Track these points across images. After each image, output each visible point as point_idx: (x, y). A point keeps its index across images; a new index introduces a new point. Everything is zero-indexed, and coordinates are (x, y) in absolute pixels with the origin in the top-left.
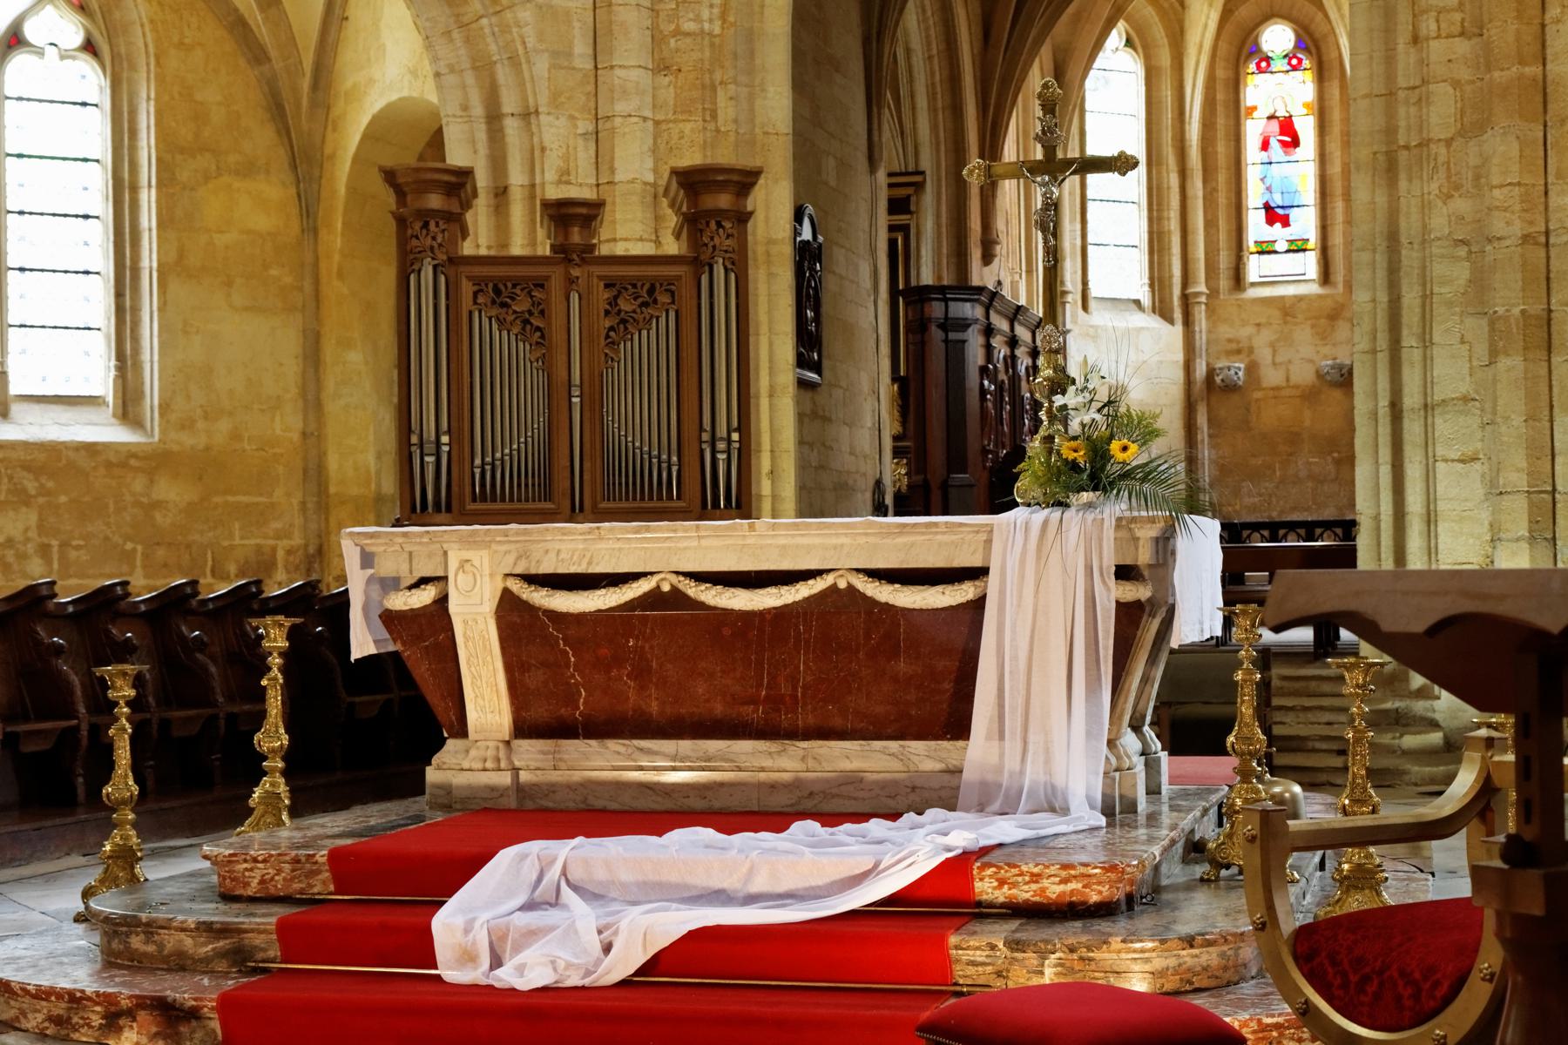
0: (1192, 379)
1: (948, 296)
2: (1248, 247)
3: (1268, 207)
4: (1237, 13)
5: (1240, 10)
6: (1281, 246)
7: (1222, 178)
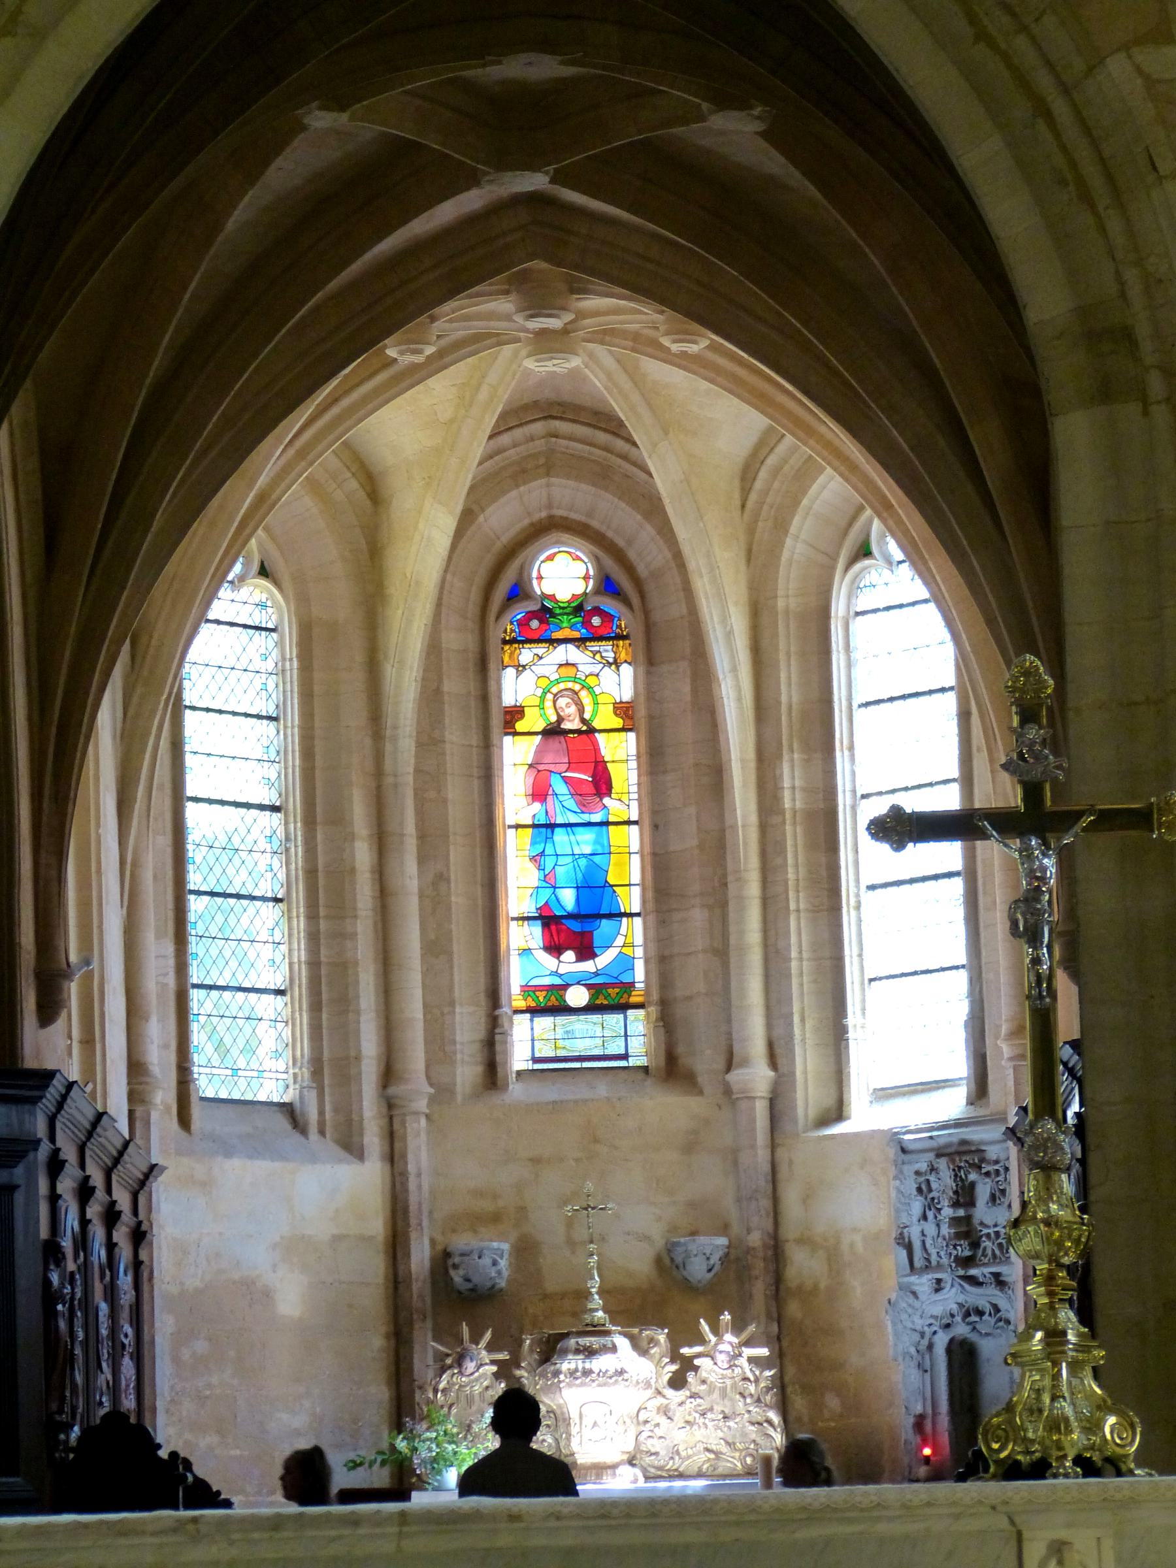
0: (401, 1268)
3: (548, 919)
4: (481, 518)
6: (577, 996)
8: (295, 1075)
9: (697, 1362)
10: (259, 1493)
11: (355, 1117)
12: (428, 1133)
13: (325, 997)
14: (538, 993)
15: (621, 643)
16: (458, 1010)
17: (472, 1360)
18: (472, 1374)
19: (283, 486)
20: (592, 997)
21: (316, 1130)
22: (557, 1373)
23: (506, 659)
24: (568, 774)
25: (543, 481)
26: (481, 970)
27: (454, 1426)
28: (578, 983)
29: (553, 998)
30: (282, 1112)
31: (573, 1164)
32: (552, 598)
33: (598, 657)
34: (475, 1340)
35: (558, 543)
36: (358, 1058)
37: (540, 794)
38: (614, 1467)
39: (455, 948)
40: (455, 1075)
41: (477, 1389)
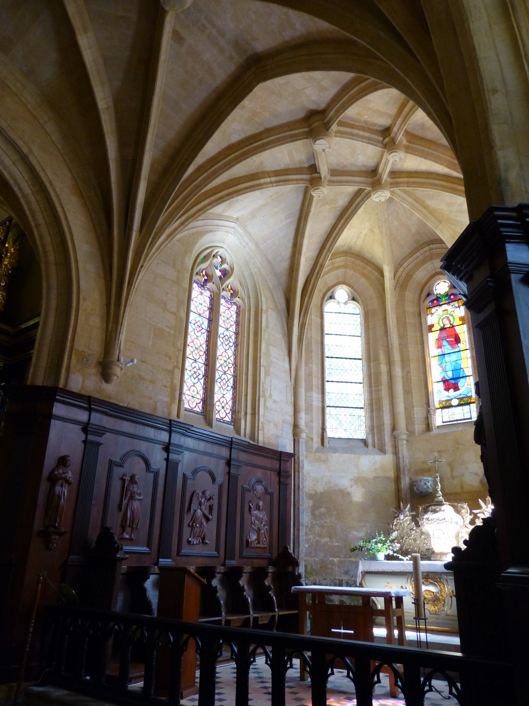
1: (92, 406)
2: (434, 404)
3: (445, 381)
4: (414, 276)
5: (416, 274)
7: (413, 366)
8: (366, 431)
9: (478, 515)
10: (345, 557)
11: (383, 442)
12: (407, 446)
13: (374, 408)
14: (443, 403)
15: (460, 301)
16: (415, 408)
17: (402, 515)
18: (403, 519)
19: (325, 260)
20: (460, 401)
21: (371, 446)
22: (423, 519)
24: (447, 340)
25: (430, 262)
26: (424, 398)
27: (383, 537)
28: (455, 398)
29: (447, 403)
30: (361, 441)
31: (451, 451)
32: (440, 294)
33: (453, 306)
34: (405, 507)
35: (439, 279)
36: (383, 424)
37: (440, 347)
38: (446, 554)
39: (413, 391)
40: (415, 428)
41: (406, 524)
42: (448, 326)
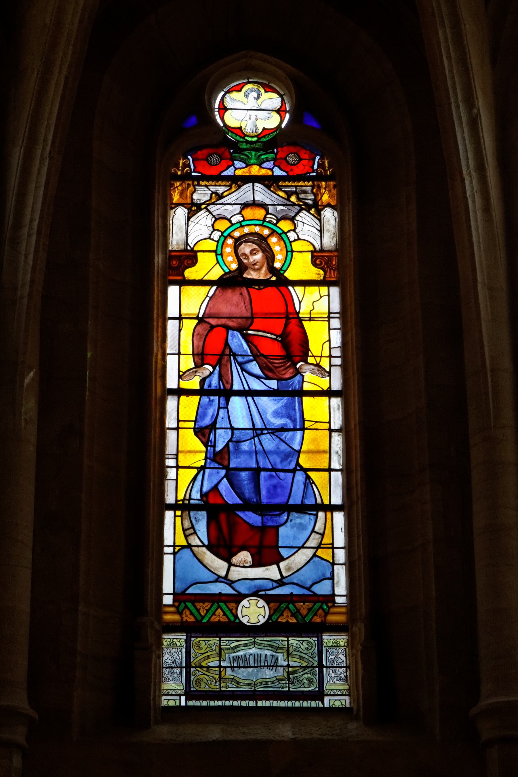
14: (199, 605)
23: (176, 198)
33: (293, 199)
42: (262, 275)
